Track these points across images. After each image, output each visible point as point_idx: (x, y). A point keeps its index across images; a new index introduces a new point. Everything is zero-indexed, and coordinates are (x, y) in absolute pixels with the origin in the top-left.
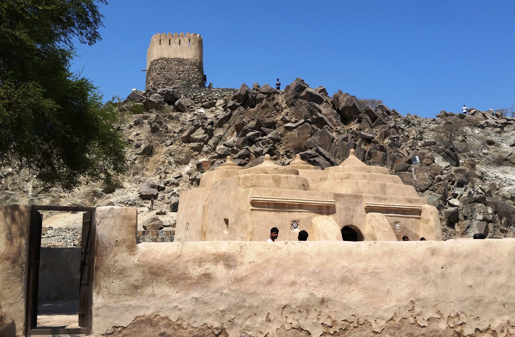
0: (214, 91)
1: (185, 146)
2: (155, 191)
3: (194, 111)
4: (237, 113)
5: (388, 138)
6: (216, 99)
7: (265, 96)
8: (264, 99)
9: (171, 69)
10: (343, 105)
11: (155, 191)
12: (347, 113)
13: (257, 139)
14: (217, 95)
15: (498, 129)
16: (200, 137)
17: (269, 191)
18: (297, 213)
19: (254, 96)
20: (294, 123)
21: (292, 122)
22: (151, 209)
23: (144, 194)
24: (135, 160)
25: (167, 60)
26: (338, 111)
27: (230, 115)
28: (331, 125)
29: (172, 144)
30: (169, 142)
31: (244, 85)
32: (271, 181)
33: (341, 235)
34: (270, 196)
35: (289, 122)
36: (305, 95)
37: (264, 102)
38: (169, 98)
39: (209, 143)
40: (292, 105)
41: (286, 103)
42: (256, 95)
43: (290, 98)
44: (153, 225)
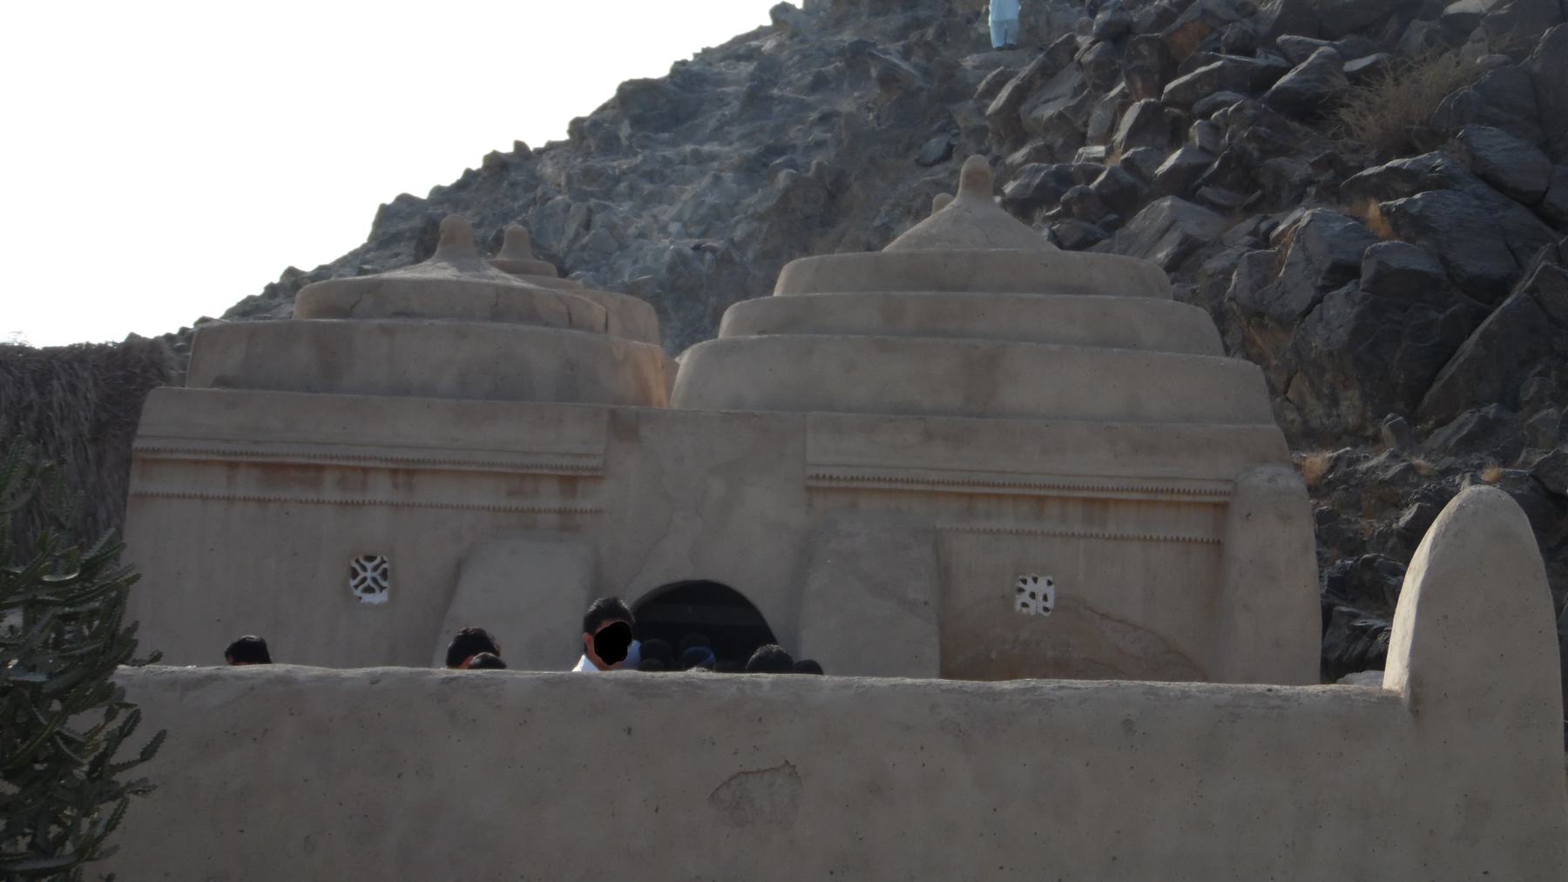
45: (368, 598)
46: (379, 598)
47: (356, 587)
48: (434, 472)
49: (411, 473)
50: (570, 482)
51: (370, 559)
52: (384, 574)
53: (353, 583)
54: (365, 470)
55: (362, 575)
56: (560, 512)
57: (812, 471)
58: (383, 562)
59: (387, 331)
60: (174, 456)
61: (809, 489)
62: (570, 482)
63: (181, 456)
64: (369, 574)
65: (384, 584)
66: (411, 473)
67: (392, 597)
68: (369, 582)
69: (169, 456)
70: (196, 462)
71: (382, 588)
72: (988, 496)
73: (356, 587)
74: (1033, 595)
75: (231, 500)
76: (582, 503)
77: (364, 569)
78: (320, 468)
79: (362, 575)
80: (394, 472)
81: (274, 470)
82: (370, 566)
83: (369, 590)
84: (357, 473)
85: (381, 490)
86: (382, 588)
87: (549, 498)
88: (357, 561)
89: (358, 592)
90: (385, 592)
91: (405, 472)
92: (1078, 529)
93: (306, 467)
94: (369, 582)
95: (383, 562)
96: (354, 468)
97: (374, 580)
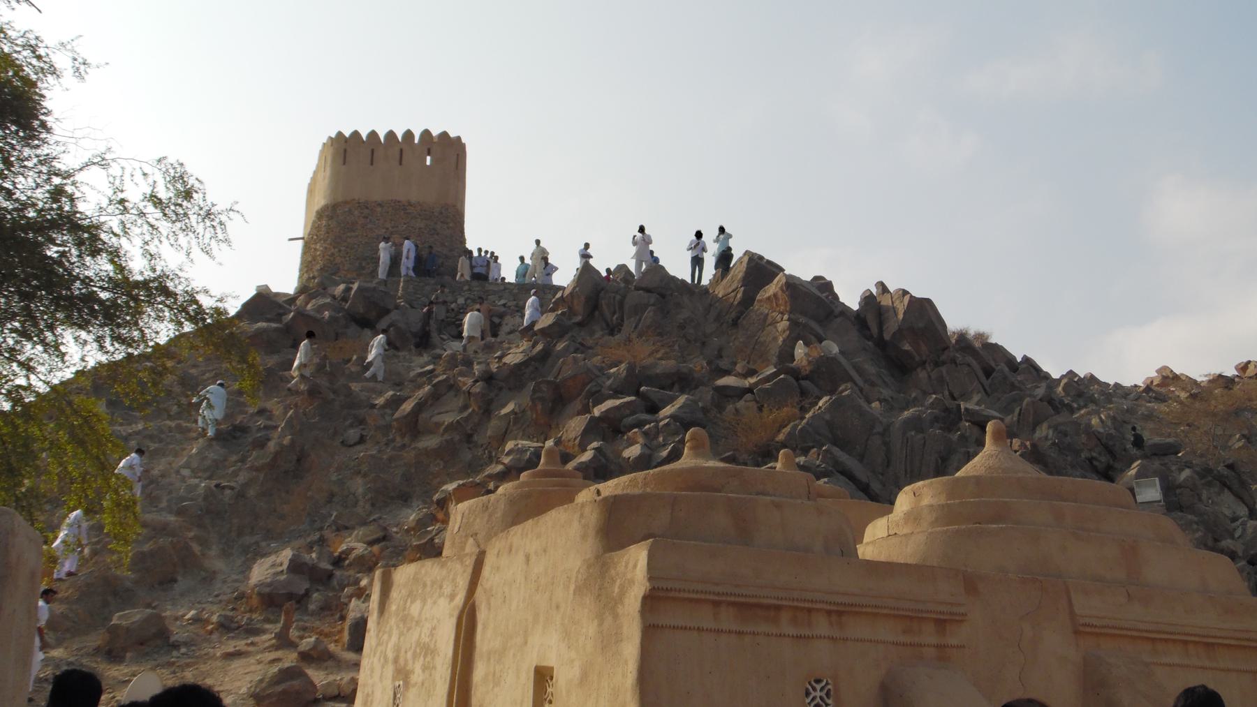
0: (495, 293)
1: (404, 446)
2: (302, 585)
3: (434, 347)
4: (566, 349)
5: (1045, 425)
6: (501, 316)
7: (653, 298)
11: (302, 585)
12: (907, 347)
13: (630, 420)
14: (503, 302)
16: (448, 419)
19: (618, 297)
20: (745, 376)
22: (284, 641)
23: (267, 590)
24: (246, 485)
26: (881, 343)
27: (545, 355)
28: (861, 383)
29: (362, 440)
30: (353, 434)
35: (727, 373)
37: (649, 315)
38: (361, 310)
39: (475, 438)
42: (624, 297)
44: (284, 692)
48: (857, 613)
49: (840, 613)
51: (818, 681)
52: (828, 694)
53: (808, 700)
54: (810, 610)
56: (938, 646)
57: (1082, 621)
58: (827, 684)
59: (778, 506)
60: (682, 595)
61: (1076, 632)
62: (941, 624)
63: (686, 595)
64: (818, 694)
65: (829, 702)
66: (840, 613)
69: (677, 595)
70: (691, 600)
72: (1166, 640)
75: (719, 631)
76: (953, 641)
77: (814, 689)
78: (778, 608)
80: (829, 613)
81: (747, 608)
82: (818, 687)
84: (802, 612)
85: (822, 626)
87: (929, 636)
91: (839, 613)
93: (768, 607)
95: (827, 684)
96: (802, 609)
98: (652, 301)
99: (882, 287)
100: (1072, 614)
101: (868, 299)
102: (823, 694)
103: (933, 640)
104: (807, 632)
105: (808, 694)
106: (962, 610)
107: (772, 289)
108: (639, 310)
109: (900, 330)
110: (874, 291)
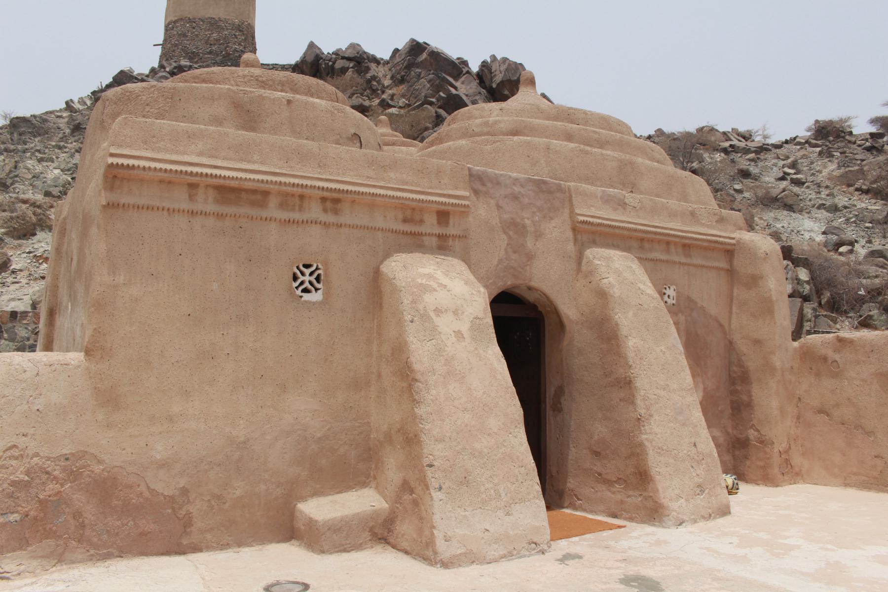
8: (348, 68)
9: (197, 35)
10: (498, 78)
15: (752, 156)
17: (191, 136)
18: (315, 230)
19: (330, 63)
21: (400, 107)
25: (190, 21)
31: (312, 45)
32: (221, 109)
33: (489, 321)
34: (201, 154)
35: (391, 106)
36: (426, 59)
40: (402, 81)
41: (392, 78)
42: (334, 63)
43: (398, 68)
45: (306, 297)
46: (315, 297)
47: (297, 288)
49: (337, 201)
50: (443, 216)
51: (307, 266)
52: (318, 279)
55: (302, 278)
56: (439, 236)
57: (581, 218)
58: (317, 269)
64: (307, 278)
67: (327, 295)
68: (307, 285)
71: (317, 290)
73: (297, 288)
74: (669, 296)
75: (193, 213)
77: (303, 274)
78: (266, 193)
79: (302, 278)
80: (324, 200)
82: (307, 271)
83: (306, 291)
84: (293, 198)
86: (317, 290)
88: (298, 268)
89: (299, 292)
90: (319, 292)
91: (333, 201)
92: (683, 260)
94: (307, 285)
95: (317, 269)
97: (311, 283)
98: (351, 65)
99: (494, 58)
100: (572, 213)
101: (484, 65)
102: (313, 278)
103: (437, 230)
104: (297, 216)
105: (295, 278)
106: (467, 203)
107: (424, 55)
108: (344, 70)
109: (502, 82)
110: (489, 60)
